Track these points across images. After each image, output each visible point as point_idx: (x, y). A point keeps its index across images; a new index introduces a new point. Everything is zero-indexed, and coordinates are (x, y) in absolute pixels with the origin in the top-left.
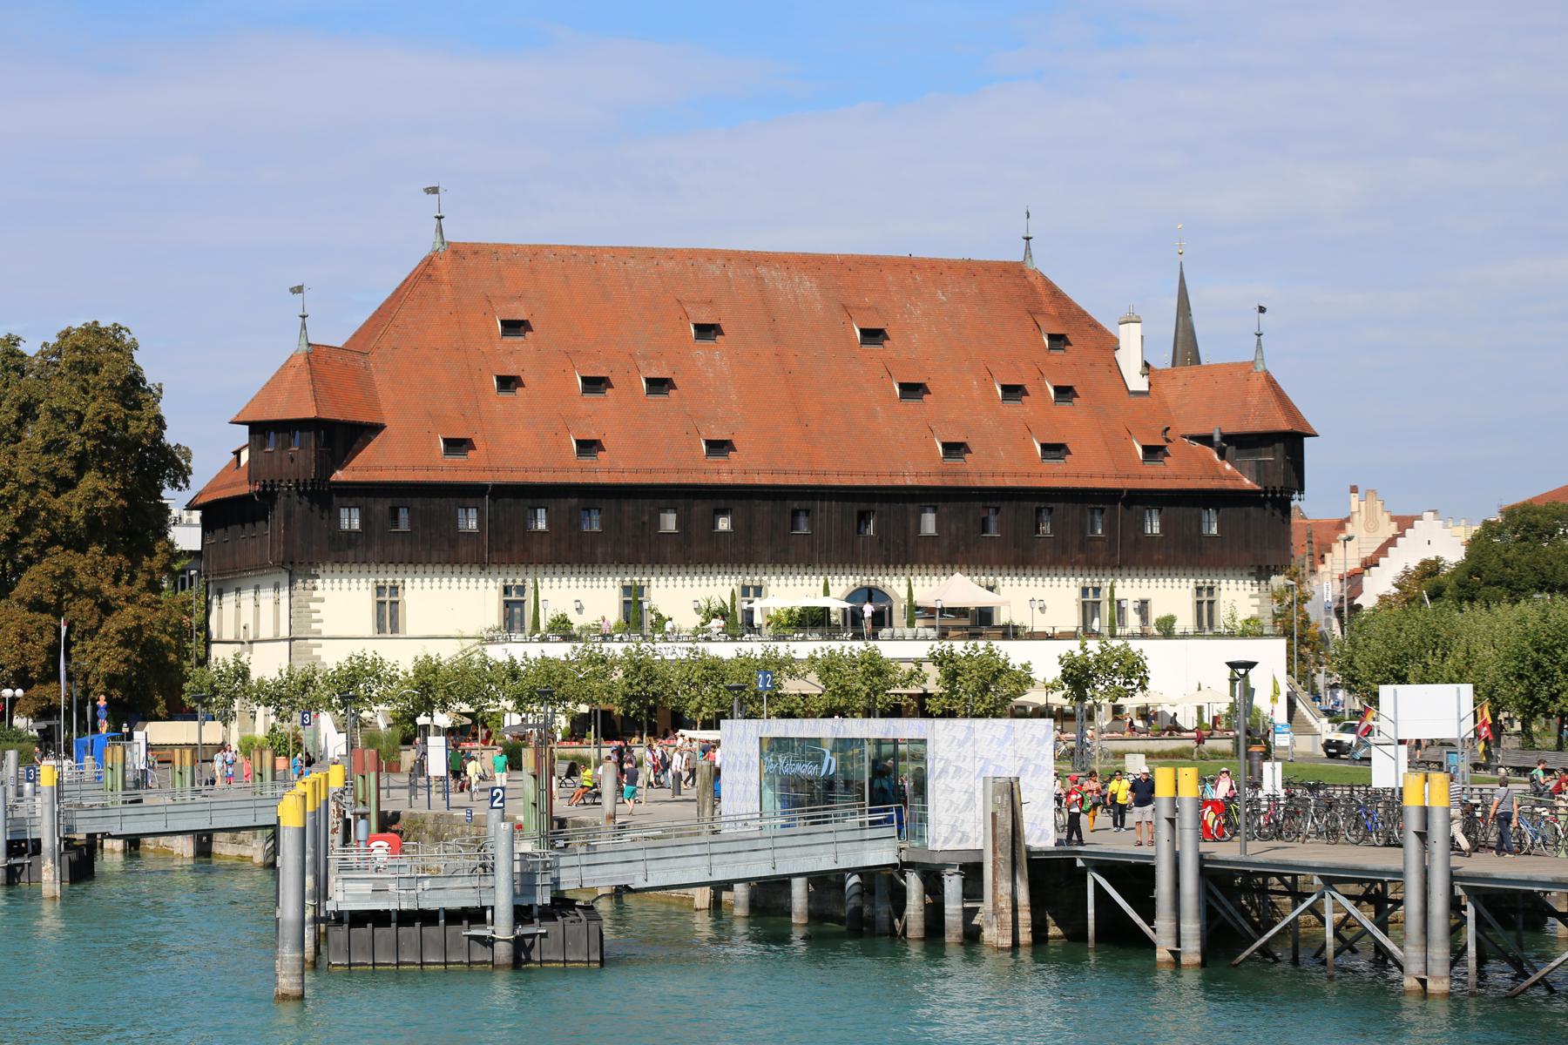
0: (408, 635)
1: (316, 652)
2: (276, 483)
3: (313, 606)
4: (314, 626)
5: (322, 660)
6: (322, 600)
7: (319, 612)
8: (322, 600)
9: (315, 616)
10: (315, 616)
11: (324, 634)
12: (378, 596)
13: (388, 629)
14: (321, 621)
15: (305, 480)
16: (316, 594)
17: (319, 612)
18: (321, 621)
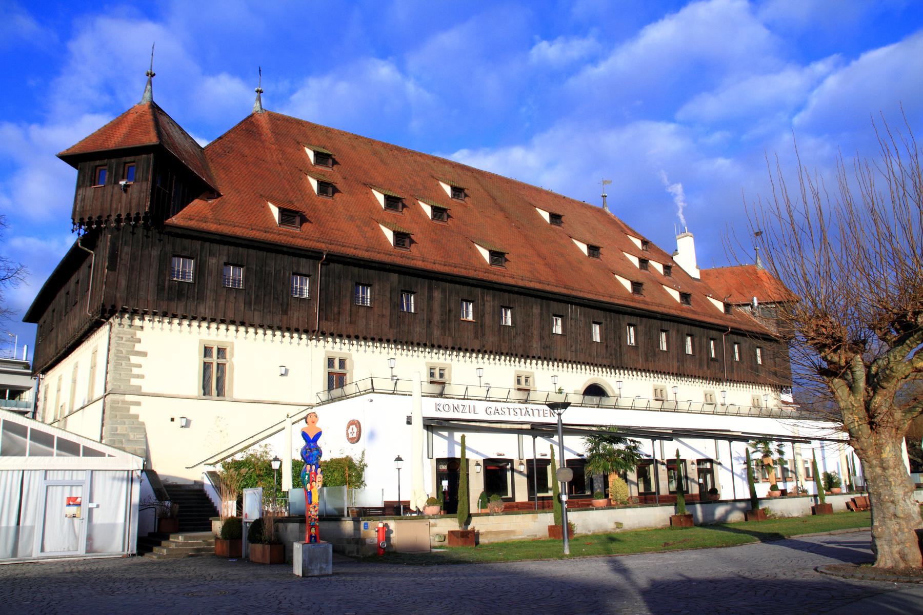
0: (236, 396)
1: (133, 410)
2: (103, 220)
3: (134, 359)
4: (134, 382)
5: (141, 419)
6: (144, 354)
7: (140, 366)
8: (144, 354)
9: (135, 371)
10: (135, 371)
11: (144, 390)
12: (205, 356)
13: (214, 392)
14: (142, 377)
15: (138, 214)
16: (138, 347)
17: (140, 366)
18: (142, 377)
